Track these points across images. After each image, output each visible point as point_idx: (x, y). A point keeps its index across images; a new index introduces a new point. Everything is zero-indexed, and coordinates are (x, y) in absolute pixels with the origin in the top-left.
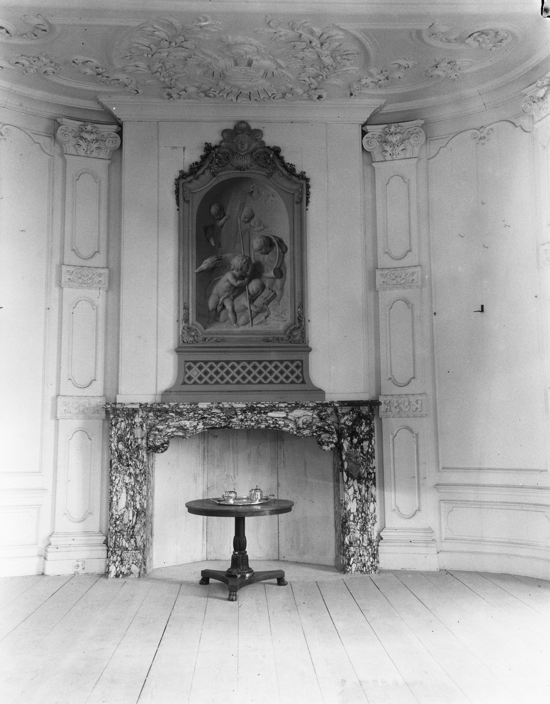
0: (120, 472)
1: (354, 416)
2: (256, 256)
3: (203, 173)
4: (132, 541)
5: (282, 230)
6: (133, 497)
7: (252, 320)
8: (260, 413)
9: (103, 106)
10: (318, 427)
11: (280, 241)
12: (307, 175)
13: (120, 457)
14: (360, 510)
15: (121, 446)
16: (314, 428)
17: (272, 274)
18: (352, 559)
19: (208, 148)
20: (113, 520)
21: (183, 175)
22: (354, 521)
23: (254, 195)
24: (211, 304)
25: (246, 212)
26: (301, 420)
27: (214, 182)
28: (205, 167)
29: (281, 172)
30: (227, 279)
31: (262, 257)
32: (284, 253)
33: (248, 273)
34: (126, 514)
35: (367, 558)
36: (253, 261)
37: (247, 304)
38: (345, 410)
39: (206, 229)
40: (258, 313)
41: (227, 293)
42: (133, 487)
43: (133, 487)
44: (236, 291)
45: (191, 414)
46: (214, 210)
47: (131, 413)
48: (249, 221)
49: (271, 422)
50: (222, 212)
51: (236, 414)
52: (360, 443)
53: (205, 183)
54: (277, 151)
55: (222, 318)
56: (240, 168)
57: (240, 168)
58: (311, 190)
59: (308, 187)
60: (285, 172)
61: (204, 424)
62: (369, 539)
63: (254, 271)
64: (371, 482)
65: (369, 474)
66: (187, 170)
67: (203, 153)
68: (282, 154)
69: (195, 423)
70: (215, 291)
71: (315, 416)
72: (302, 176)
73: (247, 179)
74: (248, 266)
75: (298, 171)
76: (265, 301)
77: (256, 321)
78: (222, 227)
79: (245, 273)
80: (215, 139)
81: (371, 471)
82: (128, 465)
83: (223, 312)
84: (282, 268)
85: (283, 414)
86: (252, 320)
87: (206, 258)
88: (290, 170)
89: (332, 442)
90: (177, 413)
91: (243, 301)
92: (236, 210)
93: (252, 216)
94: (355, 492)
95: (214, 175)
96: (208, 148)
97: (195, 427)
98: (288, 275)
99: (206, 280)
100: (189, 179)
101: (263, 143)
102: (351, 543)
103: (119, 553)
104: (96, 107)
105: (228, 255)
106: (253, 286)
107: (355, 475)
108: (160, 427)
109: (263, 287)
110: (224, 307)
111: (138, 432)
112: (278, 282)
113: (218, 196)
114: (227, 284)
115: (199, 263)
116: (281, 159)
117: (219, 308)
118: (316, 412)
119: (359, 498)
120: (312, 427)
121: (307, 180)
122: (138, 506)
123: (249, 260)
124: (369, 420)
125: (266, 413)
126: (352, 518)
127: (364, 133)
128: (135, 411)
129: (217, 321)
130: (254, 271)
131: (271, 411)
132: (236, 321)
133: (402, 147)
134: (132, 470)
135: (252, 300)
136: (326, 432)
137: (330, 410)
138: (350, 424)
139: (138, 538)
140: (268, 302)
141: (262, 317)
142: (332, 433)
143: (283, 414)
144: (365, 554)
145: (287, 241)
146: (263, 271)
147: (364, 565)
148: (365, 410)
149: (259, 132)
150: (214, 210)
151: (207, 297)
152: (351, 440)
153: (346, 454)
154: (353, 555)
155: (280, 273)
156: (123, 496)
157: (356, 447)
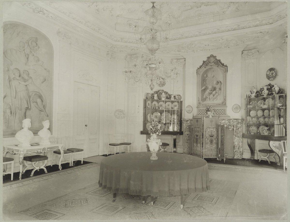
2: (215, 86)
5: (221, 79)
10: (228, 125)
11: (220, 82)
12: (227, 65)
19: (204, 62)
21: (198, 69)
22: (236, 147)
24: (204, 97)
25: (212, 76)
27: (205, 69)
28: (203, 66)
30: (208, 91)
32: (221, 84)
33: (213, 89)
37: (212, 96)
38: (235, 121)
39: (203, 80)
46: (205, 76)
53: (203, 69)
54: (219, 61)
56: (211, 66)
57: (211, 66)
59: (227, 68)
60: (222, 65)
67: (203, 63)
70: (205, 94)
72: (226, 66)
73: (213, 68)
75: (225, 65)
80: (205, 59)
88: (223, 65)
91: (212, 96)
92: (210, 75)
93: (214, 76)
94: (237, 140)
95: (205, 68)
96: (204, 62)
98: (222, 90)
100: (199, 69)
101: (216, 59)
106: (214, 92)
109: (216, 93)
110: (207, 97)
114: (208, 92)
115: (202, 88)
116: (221, 63)
117: (206, 98)
118: (228, 121)
127: (242, 53)
128: (188, 120)
129: (205, 101)
130: (215, 89)
135: (214, 96)
136: (230, 126)
137: (231, 121)
145: (222, 82)
146: (216, 89)
148: (240, 121)
149: (216, 56)
150: (205, 76)
151: (203, 95)
154: (236, 154)
155: (220, 89)
157: (237, 130)
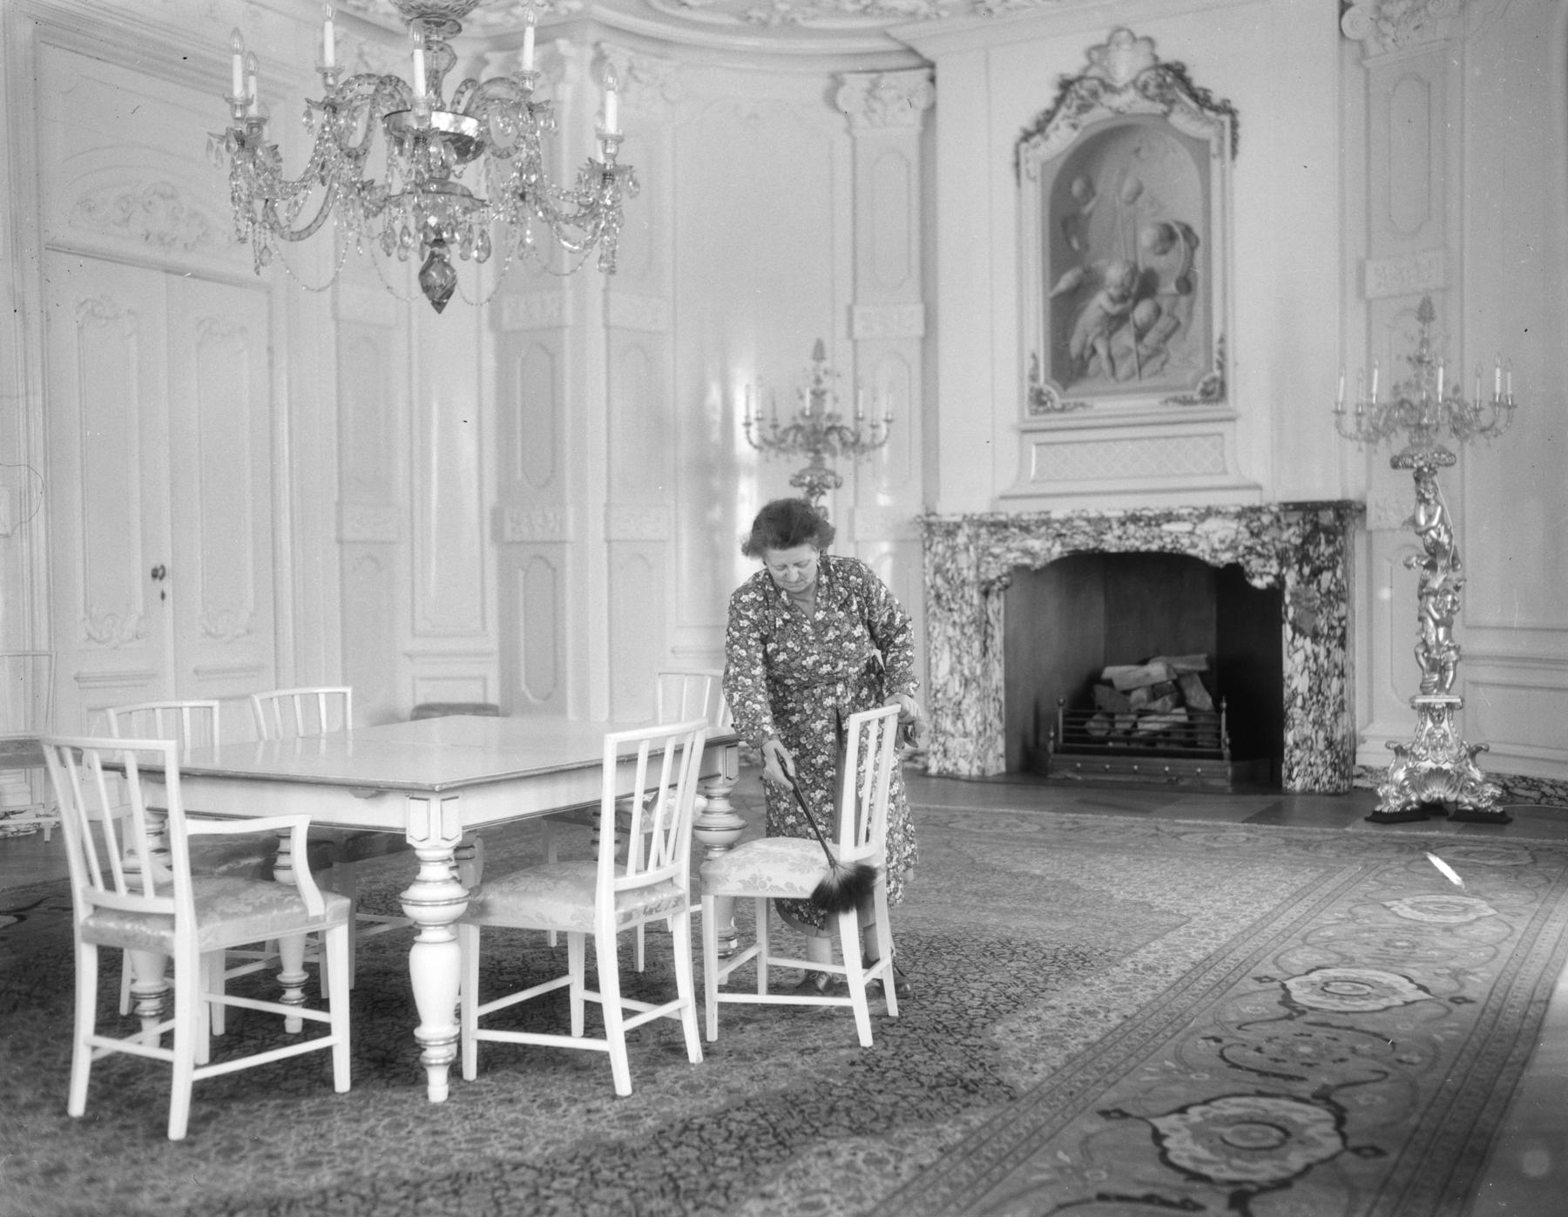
0: (940, 620)
1: (1308, 528)
3: (1057, 128)
4: (959, 723)
8: (1149, 525)
11: (1188, 231)
12: (1234, 105)
13: (938, 597)
14: (1316, 689)
15: (939, 581)
16: (1241, 549)
17: (1172, 288)
22: (1303, 708)
23: (1143, 154)
24: (1075, 346)
25: (1128, 186)
30: (1100, 303)
32: (1193, 249)
33: (1134, 290)
38: (1294, 517)
39: (1065, 225)
40: (1149, 357)
41: (1098, 330)
42: (959, 643)
43: (959, 643)
45: (1043, 529)
46: (1077, 187)
50: (1089, 190)
58: (1240, 131)
61: (1063, 545)
63: (1144, 285)
64: (1335, 642)
65: (1332, 628)
68: (1188, 74)
69: (1049, 544)
71: (1242, 529)
72: (1225, 109)
75: (1216, 99)
77: (1146, 370)
78: (1090, 214)
79: (1128, 290)
81: (1335, 623)
82: (950, 610)
85: (1187, 527)
87: (1063, 272)
91: (1126, 337)
92: (1113, 182)
93: (1138, 192)
94: (1307, 659)
97: (1049, 550)
99: (1064, 309)
103: (941, 739)
105: (1101, 263)
106: (1142, 312)
107: (1307, 628)
108: (996, 550)
109: (1158, 311)
110: (1094, 351)
111: (963, 560)
112: (1183, 300)
114: (1100, 313)
117: (1087, 353)
118: (1244, 522)
119: (1314, 668)
121: (1232, 113)
122: (966, 672)
124: (1332, 533)
125: (1158, 525)
126: (1299, 701)
131: (1169, 521)
134: (956, 617)
135: (1140, 335)
138: (1298, 541)
139: (968, 720)
140: (1167, 337)
141: (1155, 364)
142: (1270, 558)
143: (1187, 527)
148: (1327, 518)
150: (1077, 187)
153: (1292, 595)
155: (1186, 285)
157: (1309, 582)
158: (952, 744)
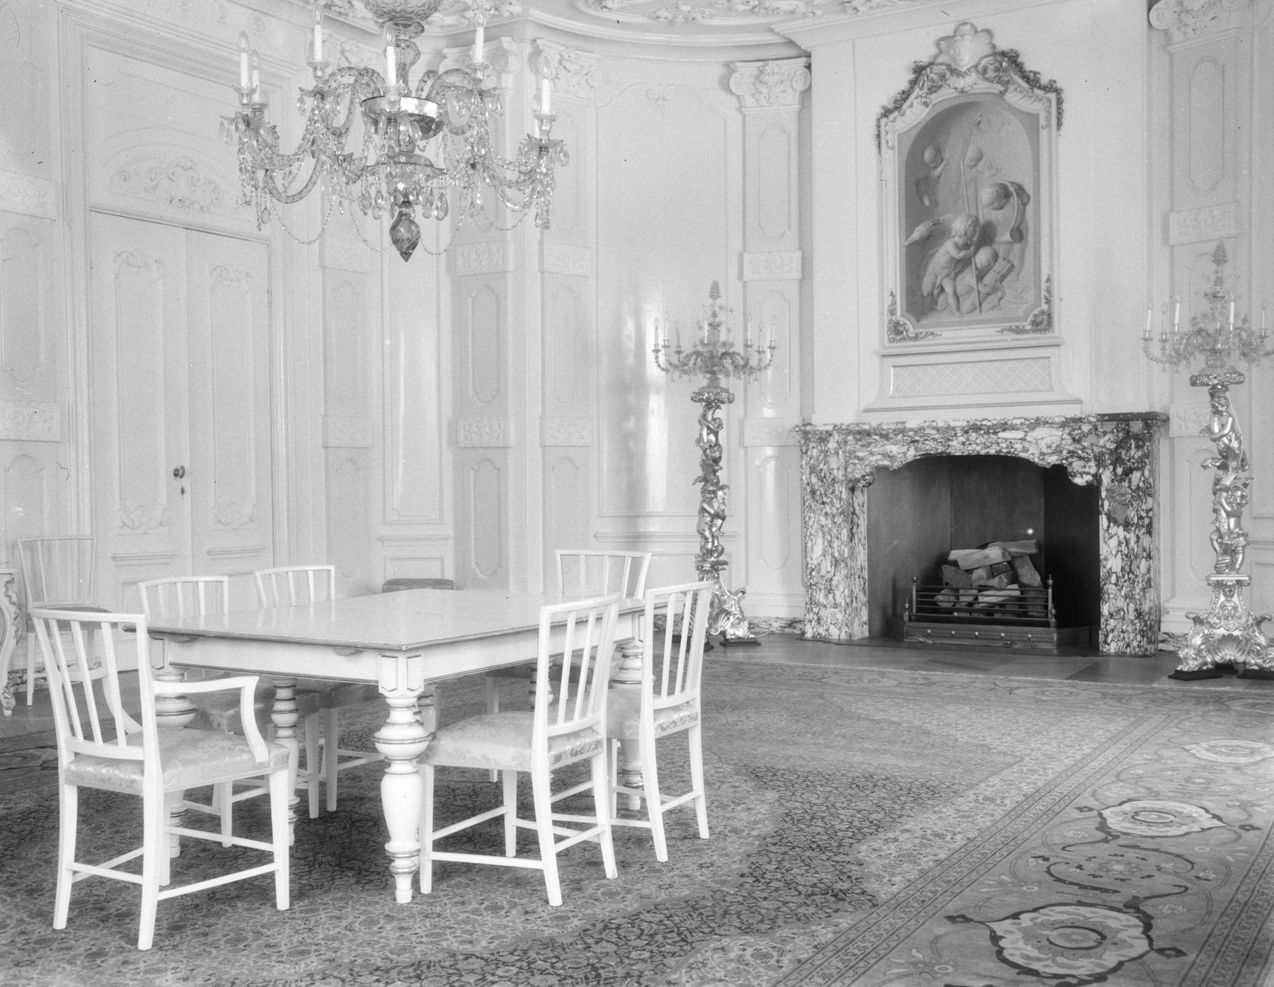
0: (814, 512)
1: (1121, 435)
3: (911, 106)
4: (831, 596)
6: (830, 542)
7: (980, 304)
8: (987, 433)
9: (783, 37)
10: (1069, 452)
11: (1020, 189)
12: (1059, 85)
13: (813, 492)
14: (1127, 569)
15: (814, 479)
16: (1065, 452)
17: (1007, 237)
18: (1111, 636)
20: (808, 571)
22: (1116, 585)
23: (983, 126)
24: (926, 285)
25: (971, 152)
26: (1044, 442)
29: (1020, 86)
30: (947, 250)
31: (994, 213)
32: (1025, 205)
33: (975, 239)
34: (823, 564)
35: (1132, 636)
36: (982, 221)
38: (1109, 426)
39: (918, 185)
40: (988, 294)
41: (946, 271)
42: (830, 530)
43: (830, 530)
44: (961, 265)
45: (900, 437)
46: (928, 155)
47: (824, 438)
48: (975, 165)
49: (1004, 445)
50: (938, 157)
51: (955, 435)
52: (1127, 475)
55: (940, 307)
58: (1064, 106)
61: (916, 449)
62: (1136, 610)
63: (984, 235)
64: (1143, 530)
65: (1141, 518)
66: (891, 106)
68: (1020, 60)
69: (905, 449)
70: (930, 269)
71: (1065, 436)
72: (1052, 88)
74: (974, 231)
75: (1044, 80)
76: (998, 277)
77: (985, 306)
78: (939, 177)
79: (971, 239)
81: (1144, 514)
82: (823, 503)
83: (941, 298)
84: (1022, 228)
85: (1020, 434)
86: (980, 304)
87: (917, 225)
89: (1088, 473)
90: (882, 436)
91: (969, 278)
92: (958, 151)
93: (980, 159)
94: (1120, 543)
97: (905, 454)
99: (917, 255)
102: (1111, 615)
103: (816, 610)
104: (778, 39)
105: (948, 216)
106: (983, 256)
107: (1120, 518)
108: (861, 454)
109: (996, 256)
110: (942, 289)
111: (834, 462)
112: (1017, 246)
113: (933, 133)
114: (947, 257)
117: (936, 292)
118: (1067, 431)
119: (1126, 552)
120: (1061, 452)
121: (1058, 91)
122: (836, 554)
123: (977, 220)
124: (1140, 440)
125: (995, 433)
126: (1113, 579)
131: (1004, 430)
132: (958, 309)
133: (1211, 15)
134: (828, 509)
135: (980, 276)
138: (1113, 446)
139: (838, 594)
140: (1003, 277)
141: (993, 299)
142: (1089, 460)
143: (1020, 434)
144: (1130, 629)
146: (995, 235)
147: (1128, 645)
148: (1136, 427)
150: (928, 155)
152: (1114, 469)
153: (1107, 490)
154: (1113, 631)
155: (1019, 234)
156: (820, 540)
157: (1122, 480)
158: (823, 613)
